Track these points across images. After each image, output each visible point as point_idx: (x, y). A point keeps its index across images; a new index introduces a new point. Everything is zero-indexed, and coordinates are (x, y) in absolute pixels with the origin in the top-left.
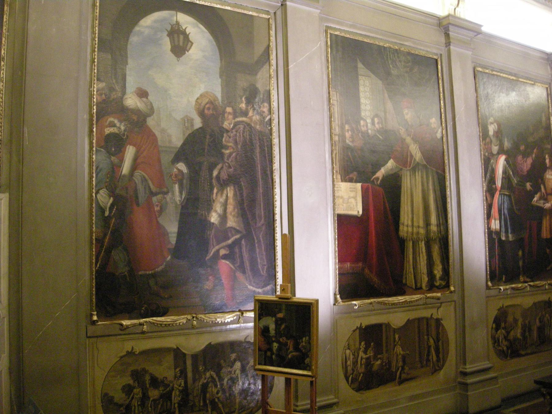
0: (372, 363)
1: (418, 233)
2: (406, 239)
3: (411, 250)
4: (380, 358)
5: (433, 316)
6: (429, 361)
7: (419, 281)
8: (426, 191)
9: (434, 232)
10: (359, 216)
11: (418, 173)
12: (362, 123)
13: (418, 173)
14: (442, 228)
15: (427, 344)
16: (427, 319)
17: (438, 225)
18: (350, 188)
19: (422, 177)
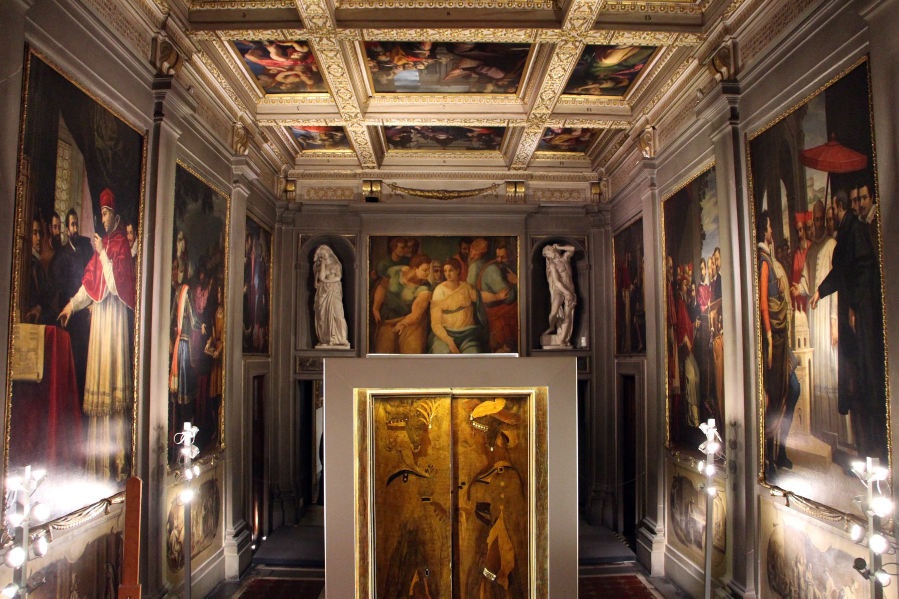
8: (115, 337)
10: (39, 382)
12: (54, 219)
17: (124, 390)
18: (31, 333)
19: (112, 315)
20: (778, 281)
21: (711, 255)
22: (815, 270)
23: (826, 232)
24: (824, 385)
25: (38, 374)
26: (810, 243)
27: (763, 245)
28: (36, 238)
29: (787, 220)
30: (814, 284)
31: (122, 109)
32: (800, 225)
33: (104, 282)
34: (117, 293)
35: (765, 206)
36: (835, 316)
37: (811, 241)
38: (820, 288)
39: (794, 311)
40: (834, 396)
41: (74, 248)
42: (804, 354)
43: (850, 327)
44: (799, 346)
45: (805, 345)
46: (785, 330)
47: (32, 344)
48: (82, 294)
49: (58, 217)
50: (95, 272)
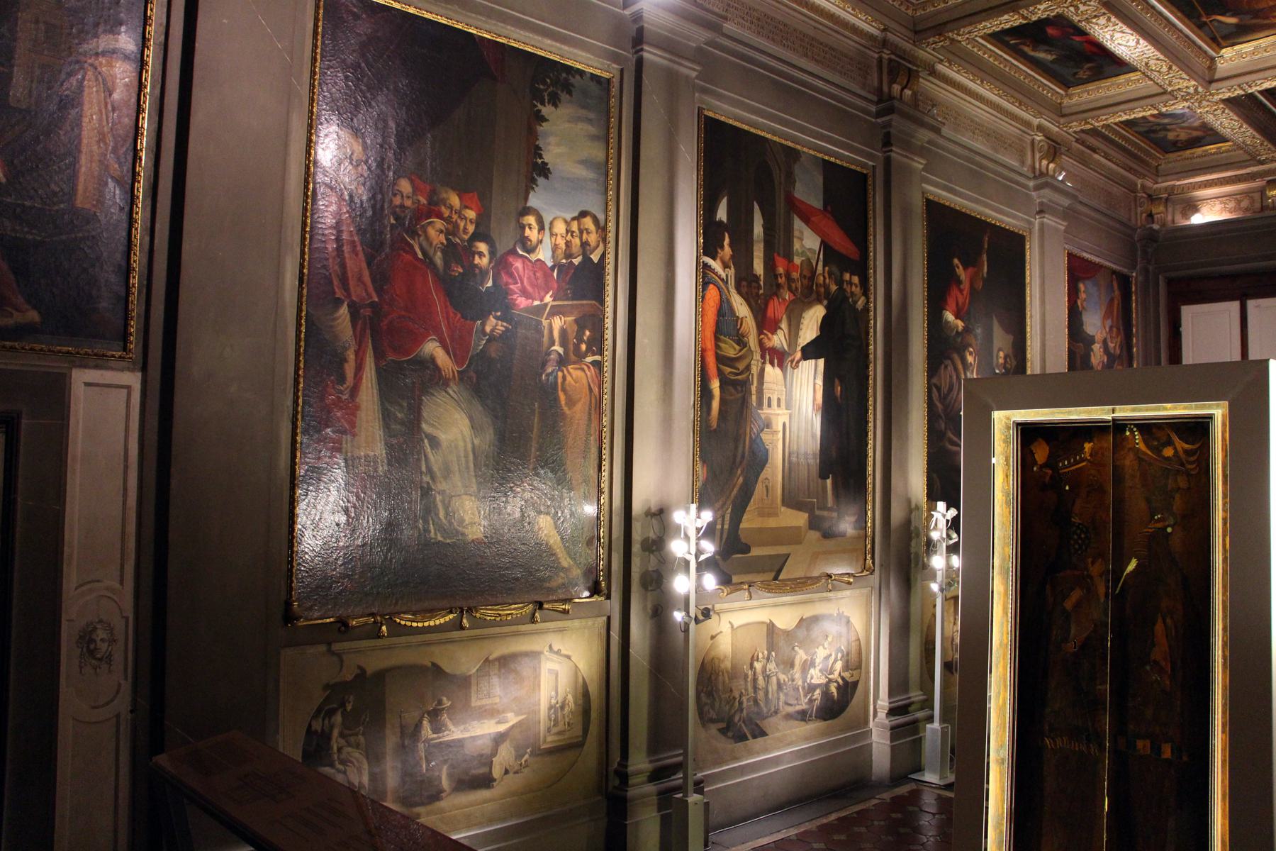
20: (737, 321)
21: (569, 217)
22: (798, 328)
23: (814, 296)
24: (802, 451)
26: (792, 298)
27: (716, 265)
29: (762, 255)
30: (796, 344)
32: (781, 270)
35: (722, 214)
36: (820, 382)
37: (795, 295)
38: (803, 349)
39: (764, 363)
40: (814, 462)
42: (779, 417)
43: (836, 398)
44: (769, 405)
45: (779, 405)
46: (745, 384)
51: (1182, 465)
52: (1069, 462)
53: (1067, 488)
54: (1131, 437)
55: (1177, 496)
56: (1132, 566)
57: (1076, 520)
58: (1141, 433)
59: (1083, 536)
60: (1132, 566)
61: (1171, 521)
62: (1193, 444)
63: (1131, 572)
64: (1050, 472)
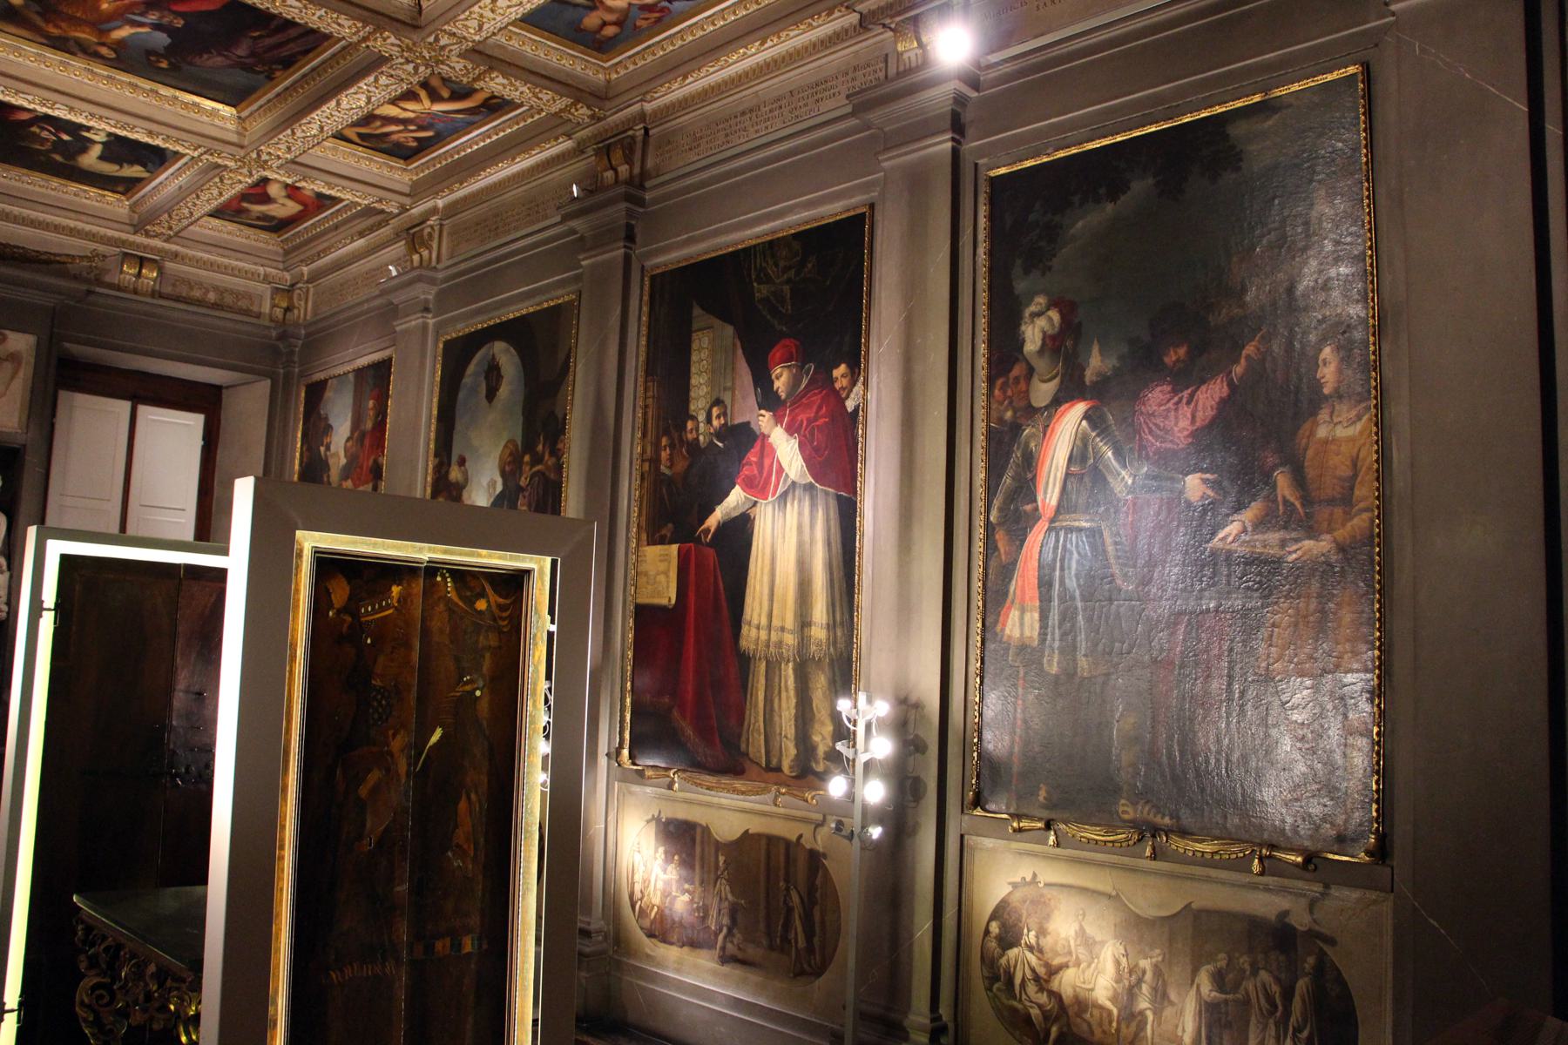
0: (674, 894)
1: (780, 644)
2: (754, 655)
3: (762, 681)
4: (687, 891)
5: (803, 841)
6: (790, 942)
7: (775, 752)
8: (807, 546)
9: (819, 644)
11: (792, 504)
12: (690, 425)
13: (792, 504)
14: (839, 633)
15: (785, 902)
16: (788, 843)
17: (831, 627)
18: (661, 555)
19: (800, 514)
25: (670, 599)
28: (664, 455)
31: (806, 214)
33: (780, 470)
34: (810, 479)
41: (720, 445)
47: (662, 567)
48: (736, 498)
49: (694, 418)
50: (760, 465)
51: (494, 620)
52: (373, 609)
53: (369, 641)
54: (442, 584)
55: (488, 655)
56: (437, 734)
57: (377, 682)
58: (454, 581)
59: (384, 702)
60: (437, 734)
61: (481, 683)
62: (506, 598)
63: (435, 744)
64: (349, 619)
